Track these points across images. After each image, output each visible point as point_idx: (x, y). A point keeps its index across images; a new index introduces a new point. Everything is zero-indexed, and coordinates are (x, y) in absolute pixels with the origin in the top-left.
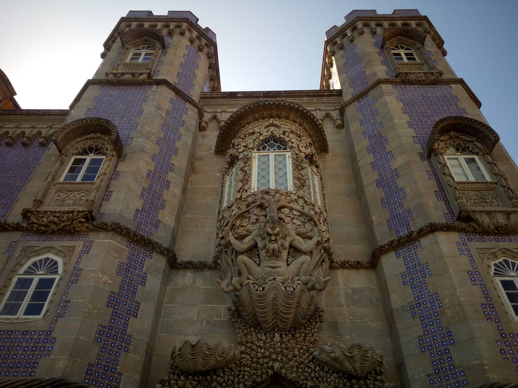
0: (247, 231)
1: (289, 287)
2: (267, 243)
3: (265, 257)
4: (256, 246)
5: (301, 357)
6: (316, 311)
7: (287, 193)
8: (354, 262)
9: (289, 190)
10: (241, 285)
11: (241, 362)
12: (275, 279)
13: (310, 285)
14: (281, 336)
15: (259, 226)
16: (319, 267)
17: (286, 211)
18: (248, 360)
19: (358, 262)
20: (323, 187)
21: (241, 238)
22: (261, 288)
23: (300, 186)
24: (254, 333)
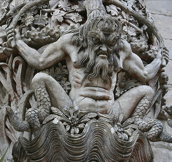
0: (49, 34)
2: (91, 57)
3: (83, 80)
4: (65, 59)
21: (37, 45)
22: (78, 131)
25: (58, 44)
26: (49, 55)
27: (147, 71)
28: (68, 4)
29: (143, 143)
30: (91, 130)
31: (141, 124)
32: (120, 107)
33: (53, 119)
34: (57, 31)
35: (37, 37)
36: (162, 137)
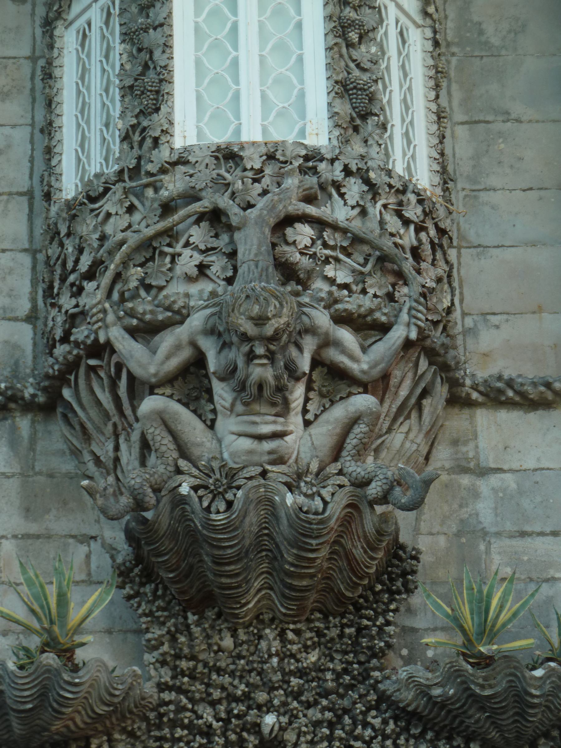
0: (168, 309)
1: (311, 497)
2: (241, 364)
3: (233, 405)
4: (199, 361)
5: (342, 697)
6: (396, 556)
7: (307, 158)
8: (534, 384)
9: (311, 141)
10: (156, 490)
11: (161, 716)
12: (264, 474)
13: (374, 490)
14: (282, 635)
15: (213, 294)
16: (408, 417)
17: (303, 233)
18: (184, 709)
19: (548, 385)
20: (438, 77)
21: (146, 331)
22: (222, 506)
23: (352, 119)
24: (196, 630)
25: (182, 332)
26: (168, 357)
27: (368, 363)
28: (209, 231)
29: (359, 508)
30: (247, 500)
31: (354, 474)
32: (313, 444)
33: (180, 485)
34: (182, 304)
35: (148, 317)
36: (390, 498)
